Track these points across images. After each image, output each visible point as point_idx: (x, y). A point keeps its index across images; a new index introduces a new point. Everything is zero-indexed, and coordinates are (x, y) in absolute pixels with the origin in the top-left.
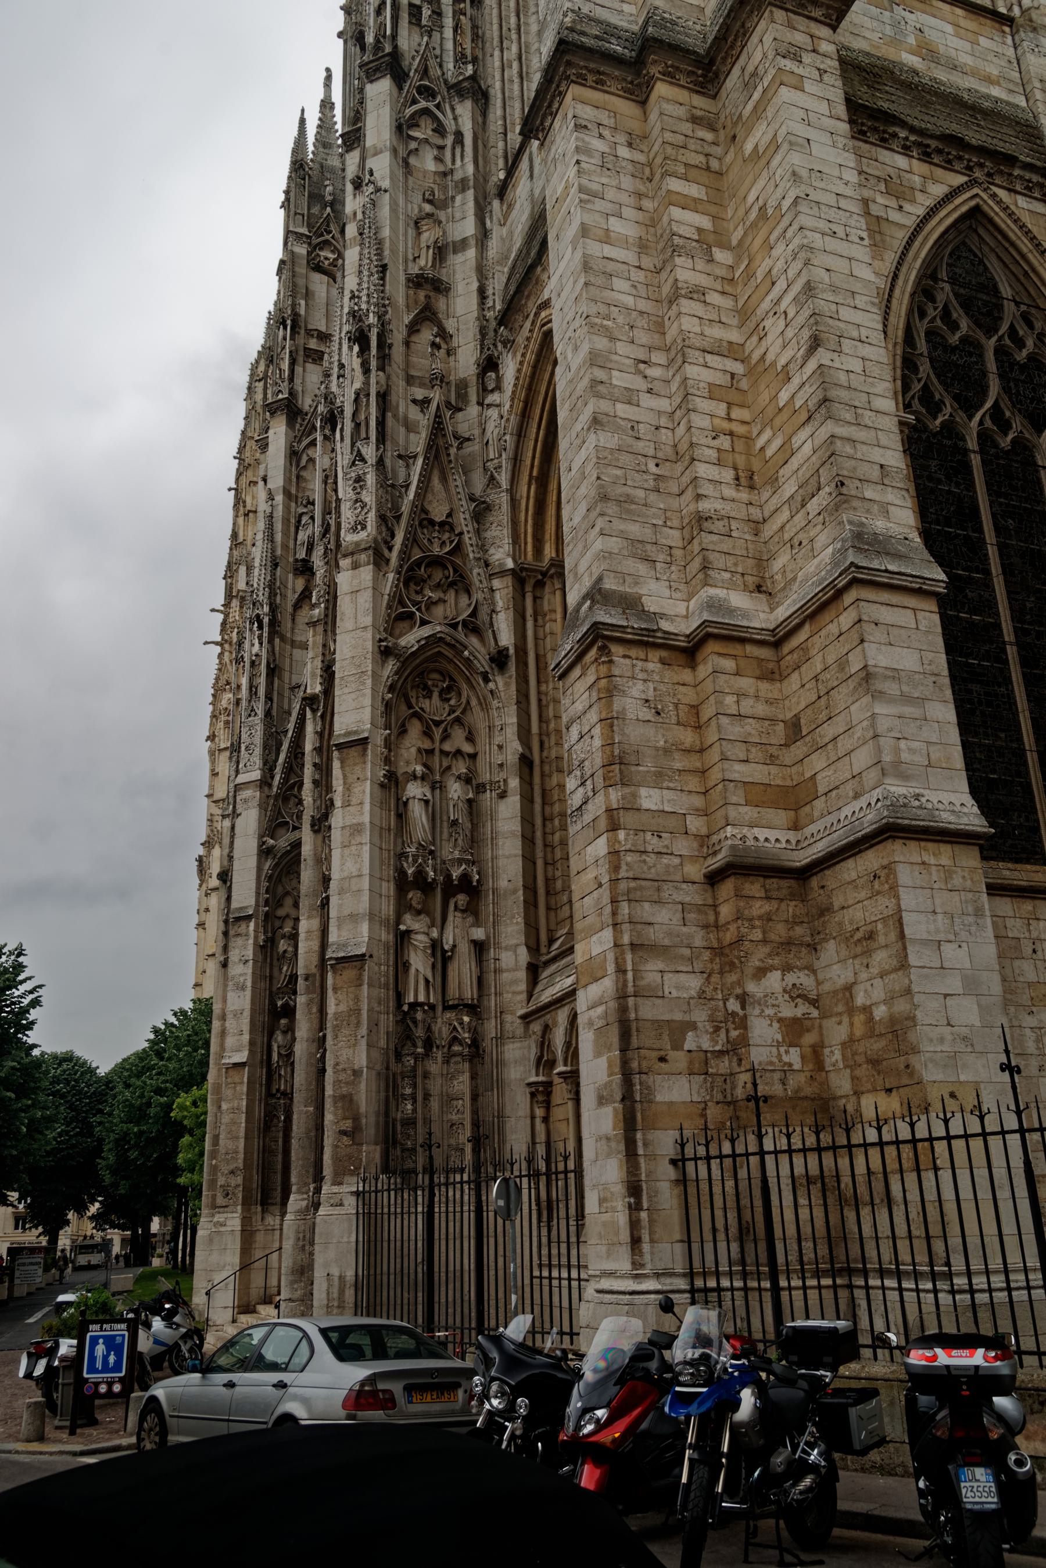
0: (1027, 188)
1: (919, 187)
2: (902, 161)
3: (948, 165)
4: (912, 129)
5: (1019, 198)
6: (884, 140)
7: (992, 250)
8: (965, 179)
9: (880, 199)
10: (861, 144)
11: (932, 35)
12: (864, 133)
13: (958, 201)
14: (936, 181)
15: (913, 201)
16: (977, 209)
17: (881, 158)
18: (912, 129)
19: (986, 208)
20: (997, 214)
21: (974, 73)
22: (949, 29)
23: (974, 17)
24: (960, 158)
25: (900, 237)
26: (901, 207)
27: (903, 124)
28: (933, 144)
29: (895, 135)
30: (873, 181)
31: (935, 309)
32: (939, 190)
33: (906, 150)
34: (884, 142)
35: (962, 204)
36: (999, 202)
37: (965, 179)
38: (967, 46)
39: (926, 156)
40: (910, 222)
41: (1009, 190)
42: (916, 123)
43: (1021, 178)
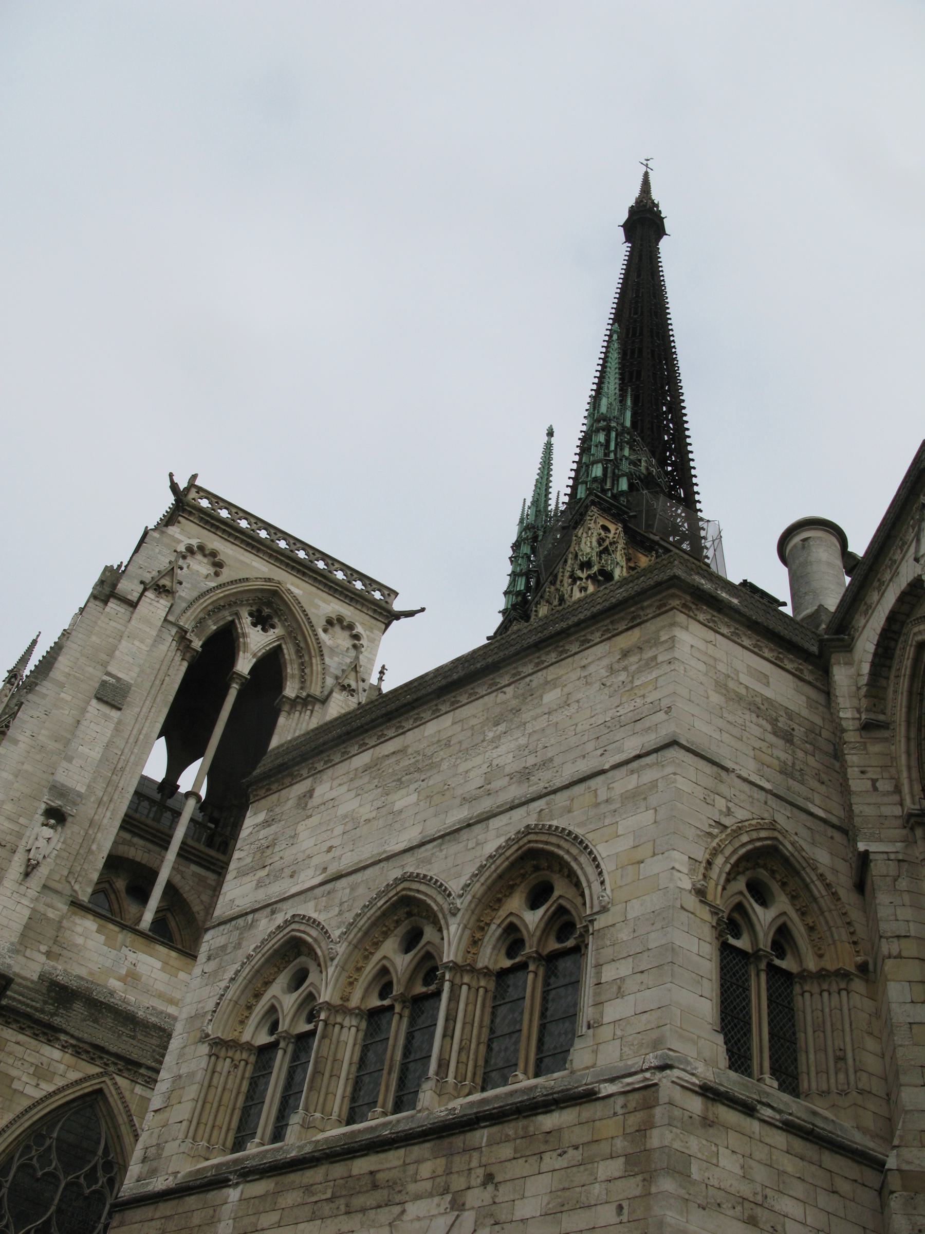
0: (146, 1081)
1: (60, 1072)
2: (56, 1054)
3: (92, 1061)
4: (72, 1036)
5: (138, 1086)
6: (49, 1041)
7: (104, 1116)
8: (101, 1070)
9: (25, 1078)
10: (32, 1041)
11: (142, 969)
12: (37, 1035)
13: (84, 1085)
14: (75, 1068)
15: (50, 1081)
16: (100, 1091)
17: (42, 1051)
18: (72, 1036)
19: (106, 1091)
20: (112, 1096)
21: (161, 996)
22: (159, 965)
23: (183, 958)
24: (101, 1058)
25: (26, 1103)
26: (38, 1085)
27: (66, 1033)
28: (86, 1047)
29: (58, 1039)
30: (26, 1065)
31: (37, 1150)
32: (74, 1076)
33: (64, 1048)
34: (49, 1042)
35: (87, 1087)
36: (118, 1088)
37: (101, 1070)
38: (165, 977)
39: (77, 1053)
40: (38, 1094)
41: (132, 1081)
42: (76, 1033)
43: (142, 1075)
